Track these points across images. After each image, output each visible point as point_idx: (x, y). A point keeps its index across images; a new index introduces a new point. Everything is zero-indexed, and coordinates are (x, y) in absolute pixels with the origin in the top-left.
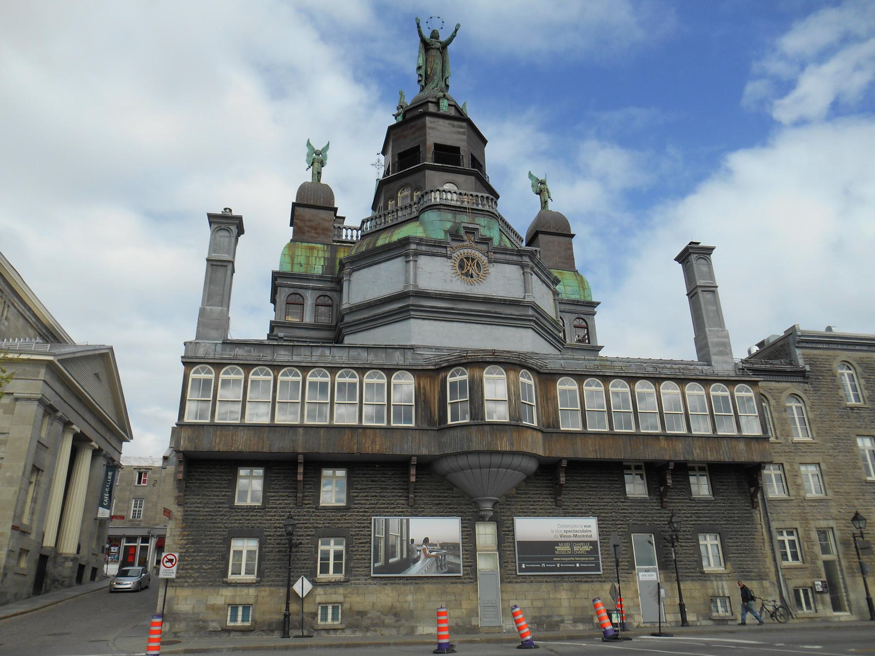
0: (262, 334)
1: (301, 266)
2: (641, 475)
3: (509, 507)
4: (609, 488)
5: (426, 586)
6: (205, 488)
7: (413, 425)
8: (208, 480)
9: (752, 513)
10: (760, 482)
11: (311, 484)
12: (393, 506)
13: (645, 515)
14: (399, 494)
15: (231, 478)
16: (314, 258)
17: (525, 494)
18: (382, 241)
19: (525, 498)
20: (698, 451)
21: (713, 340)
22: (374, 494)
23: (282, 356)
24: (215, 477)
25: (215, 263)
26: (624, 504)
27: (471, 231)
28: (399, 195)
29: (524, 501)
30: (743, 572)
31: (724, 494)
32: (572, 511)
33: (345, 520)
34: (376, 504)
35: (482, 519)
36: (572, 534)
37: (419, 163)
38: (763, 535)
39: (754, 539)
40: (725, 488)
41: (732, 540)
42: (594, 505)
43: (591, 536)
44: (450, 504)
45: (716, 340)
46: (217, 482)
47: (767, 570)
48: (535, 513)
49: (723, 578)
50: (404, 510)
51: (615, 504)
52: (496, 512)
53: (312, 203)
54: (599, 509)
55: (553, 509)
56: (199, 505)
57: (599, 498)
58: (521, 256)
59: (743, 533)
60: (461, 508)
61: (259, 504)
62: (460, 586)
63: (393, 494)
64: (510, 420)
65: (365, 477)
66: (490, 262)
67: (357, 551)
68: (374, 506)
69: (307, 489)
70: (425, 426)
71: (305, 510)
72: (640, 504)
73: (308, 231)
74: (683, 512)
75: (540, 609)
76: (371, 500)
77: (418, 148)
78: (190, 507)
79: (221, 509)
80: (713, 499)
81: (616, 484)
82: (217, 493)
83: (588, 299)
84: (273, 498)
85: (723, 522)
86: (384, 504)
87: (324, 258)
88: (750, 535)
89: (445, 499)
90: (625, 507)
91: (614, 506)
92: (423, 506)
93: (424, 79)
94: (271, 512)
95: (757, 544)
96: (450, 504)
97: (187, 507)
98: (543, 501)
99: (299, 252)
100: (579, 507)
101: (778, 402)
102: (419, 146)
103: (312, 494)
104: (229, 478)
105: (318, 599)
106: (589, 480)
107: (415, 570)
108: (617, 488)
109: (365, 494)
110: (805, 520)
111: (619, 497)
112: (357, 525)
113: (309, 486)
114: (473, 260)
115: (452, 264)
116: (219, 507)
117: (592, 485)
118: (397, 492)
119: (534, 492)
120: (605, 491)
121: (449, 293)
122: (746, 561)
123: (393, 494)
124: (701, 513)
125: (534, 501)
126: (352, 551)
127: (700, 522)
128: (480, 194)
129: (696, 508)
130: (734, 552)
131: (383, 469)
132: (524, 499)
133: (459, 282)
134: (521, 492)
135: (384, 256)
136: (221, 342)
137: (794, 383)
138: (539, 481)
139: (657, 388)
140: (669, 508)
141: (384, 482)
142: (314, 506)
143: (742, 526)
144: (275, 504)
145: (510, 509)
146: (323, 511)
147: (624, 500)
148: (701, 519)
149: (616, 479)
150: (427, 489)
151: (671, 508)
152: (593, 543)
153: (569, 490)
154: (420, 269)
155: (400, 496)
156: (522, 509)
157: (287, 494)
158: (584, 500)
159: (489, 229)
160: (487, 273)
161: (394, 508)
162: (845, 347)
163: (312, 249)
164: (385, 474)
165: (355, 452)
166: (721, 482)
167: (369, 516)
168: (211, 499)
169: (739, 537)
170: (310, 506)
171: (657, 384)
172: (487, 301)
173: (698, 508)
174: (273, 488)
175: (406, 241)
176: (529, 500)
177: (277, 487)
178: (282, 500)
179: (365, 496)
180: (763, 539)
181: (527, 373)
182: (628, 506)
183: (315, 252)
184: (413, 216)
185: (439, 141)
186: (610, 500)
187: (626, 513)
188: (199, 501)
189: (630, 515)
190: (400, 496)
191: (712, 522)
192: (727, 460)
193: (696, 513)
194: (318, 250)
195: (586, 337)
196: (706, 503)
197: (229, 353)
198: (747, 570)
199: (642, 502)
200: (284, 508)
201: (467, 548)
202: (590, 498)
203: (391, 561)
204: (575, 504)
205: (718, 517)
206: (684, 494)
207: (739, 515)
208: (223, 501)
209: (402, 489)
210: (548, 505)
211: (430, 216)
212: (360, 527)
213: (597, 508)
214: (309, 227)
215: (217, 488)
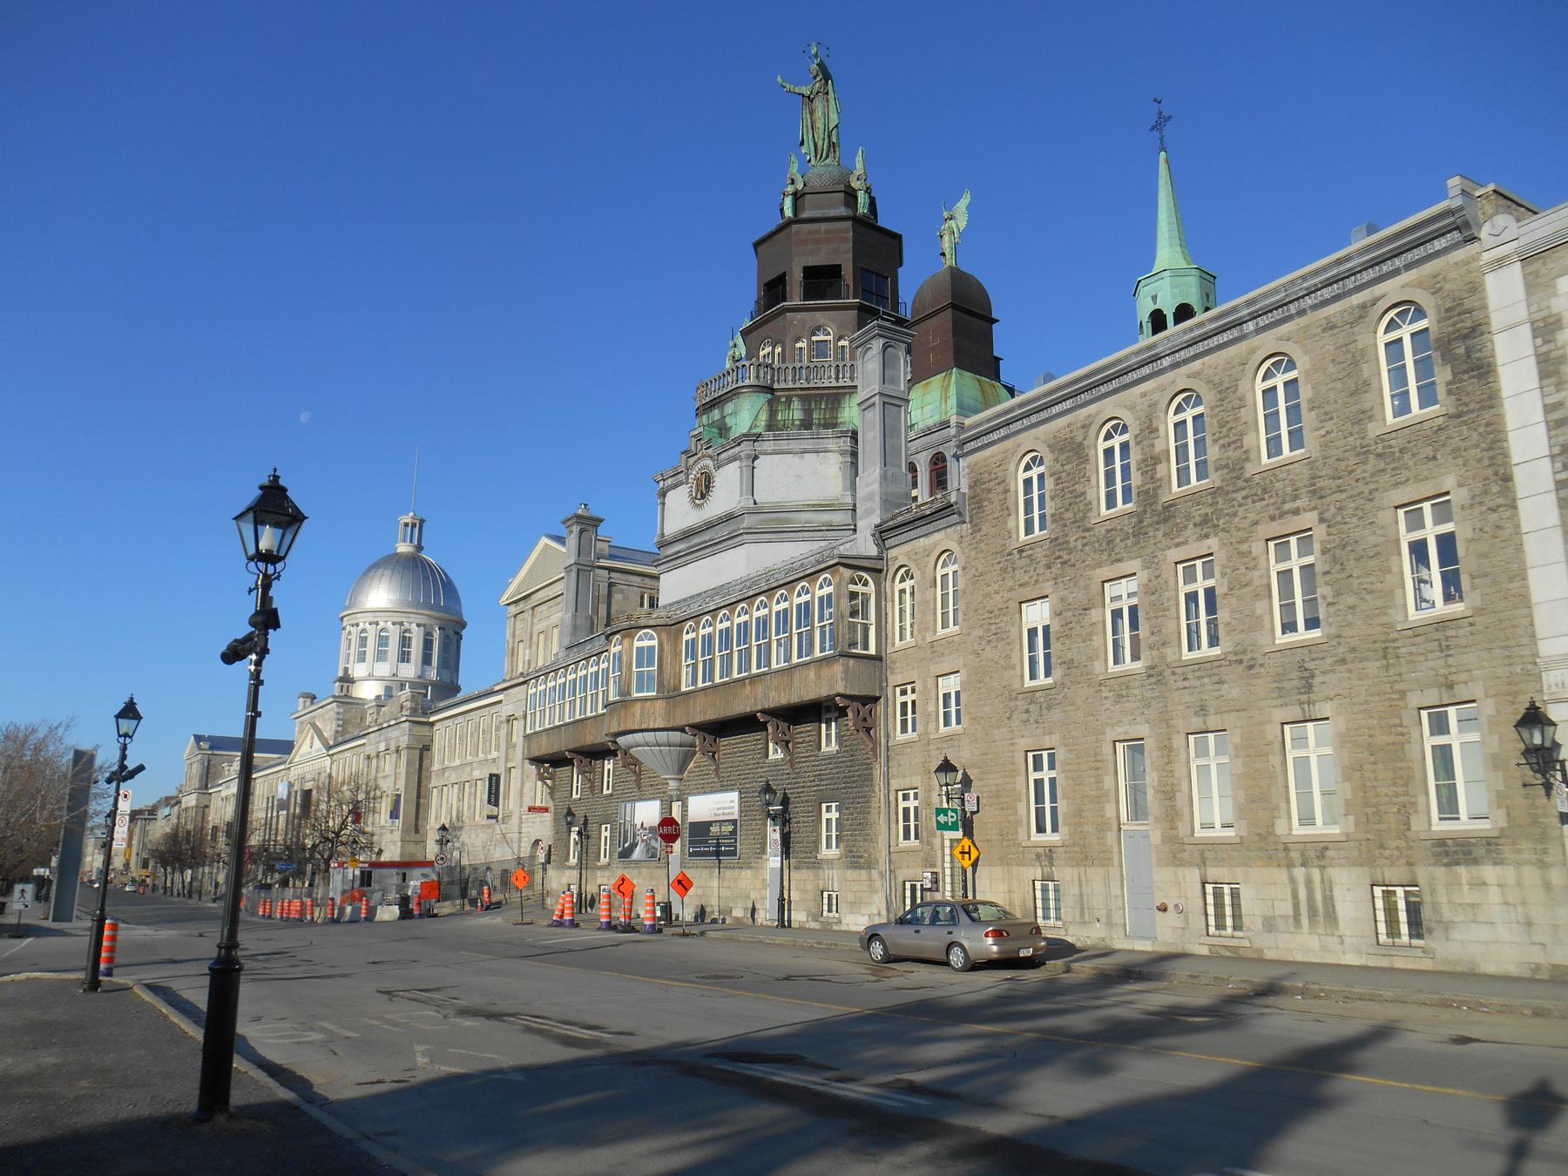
5: (643, 870)
9: (871, 769)
36: (721, 812)
43: (733, 814)
47: (878, 855)
51: (756, 771)
58: (739, 444)
62: (659, 870)
75: (700, 897)
105: (599, 881)
107: (637, 853)
130: (848, 827)
137: (949, 529)
152: (734, 822)
162: (1034, 419)
203: (626, 845)
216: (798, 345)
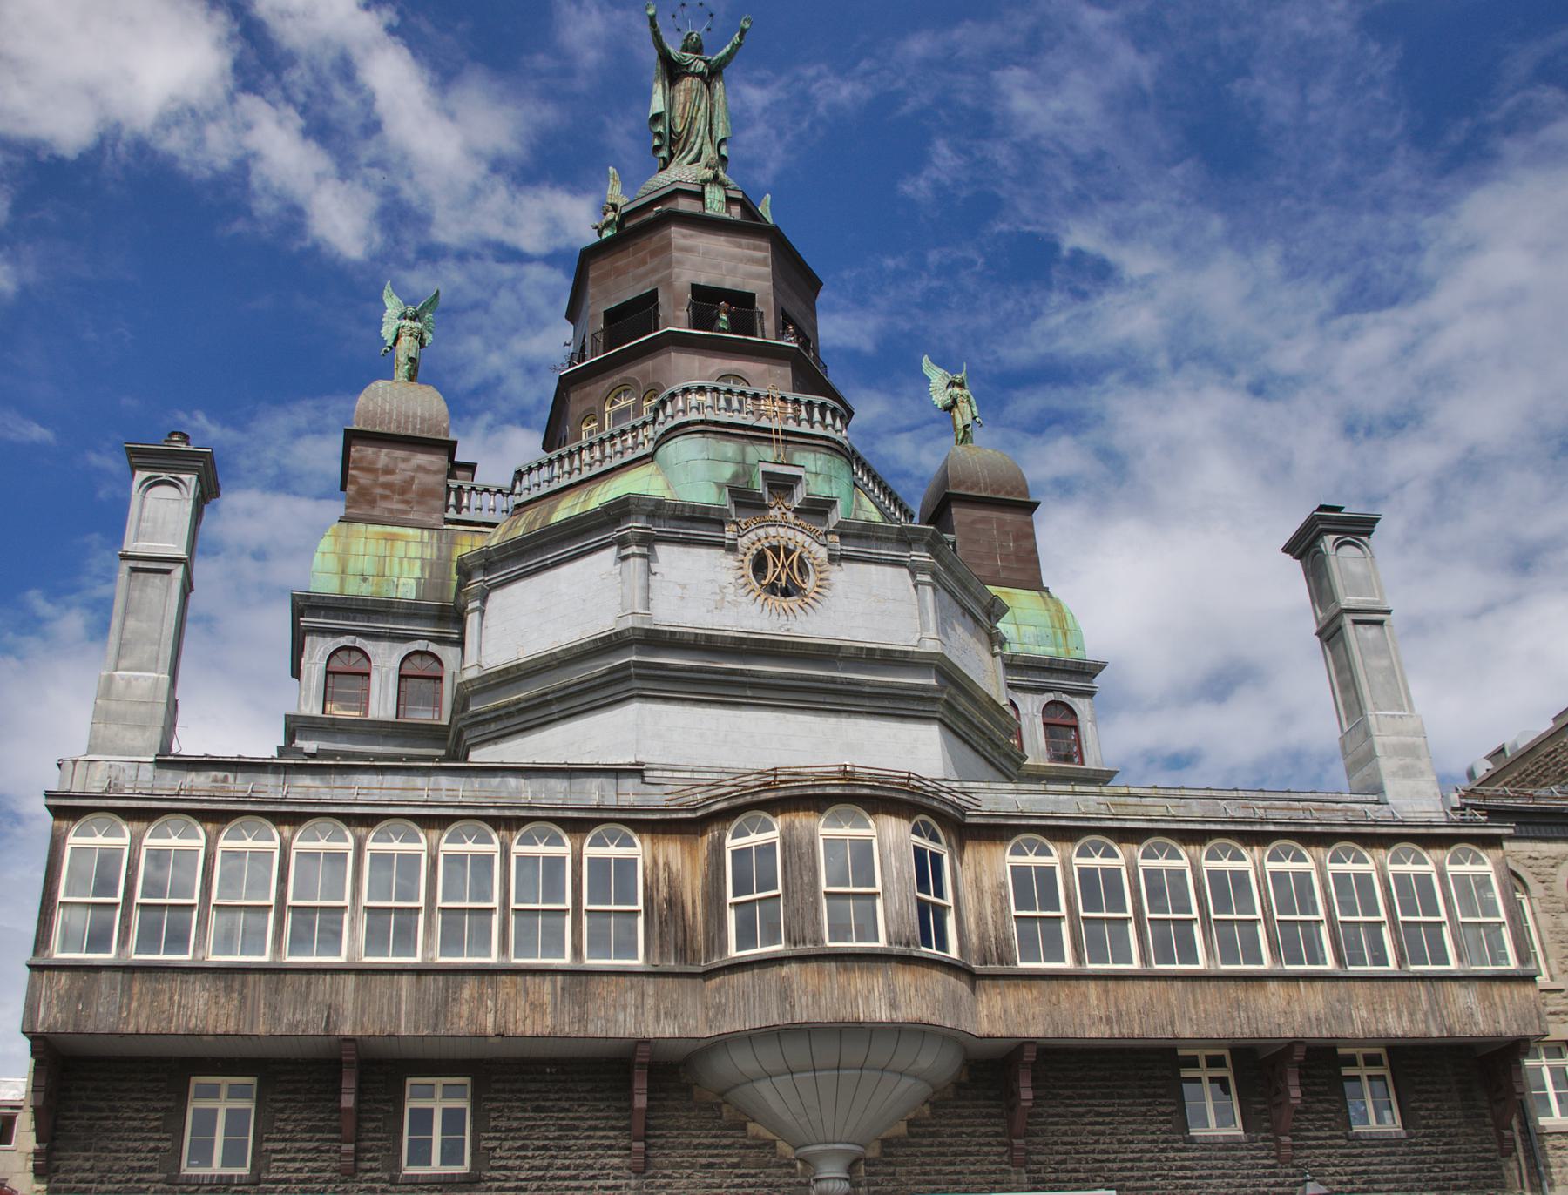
0: (265, 744)
1: (365, 580)
2: (1222, 1082)
3: (891, 1170)
4: (1145, 1114)
6: (106, 1130)
7: (638, 962)
8: (113, 1109)
9: (1500, 1168)
10: (1518, 1090)
11: (379, 1120)
12: (591, 1173)
13: (1237, 1181)
14: (607, 1142)
15: (171, 1104)
16: (396, 560)
17: (933, 1135)
18: (563, 511)
19: (932, 1145)
20: (1364, 1013)
21: (1385, 739)
22: (540, 1143)
23: (306, 788)
24: (131, 1103)
25: (141, 565)
26: (1183, 1155)
27: (782, 485)
28: (607, 409)
29: (929, 1154)
31: (1431, 1122)
32: (1053, 1176)
34: (547, 1168)
37: (656, 330)
40: (1432, 1105)
42: (1108, 1160)
45: (1394, 739)
46: (135, 1115)
48: (957, 1183)
50: (619, 1182)
51: (1162, 1156)
53: (393, 429)
54: (1120, 1170)
55: (1003, 1171)
56: (91, 1176)
57: (1120, 1142)
60: (768, 1176)
61: (245, 1171)
63: (590, 1142)
64: (889, 942)
65: (519, 1099)
66: (832, 559)
68: (541, 1173)
69: (368, 1131)
70: (672, 964)
71: (363, 1186)
72: (1223, 1154)
73: (384, 497)
74: (1332, 1169)
76: (533, 1157)
77: (653, 295)
78: (65, 1181)
79: (144, 1186)
80: (1403, 1134)
81: (1164, 1104)
82: (135, 1145)
83: (1076, 655)
84: (280, 1156)
86: (568, 1168)
87: (422, 559)
89: (726, 1152)
90: (1187, 1163)
91: (1159, 1160)
92: (669, 1172)
93: (667, 143)
97: (58, 1181)
98: (978, 1153)
99: (358, 546)
100: (1070, 1166)
102: (654, 293)
103: (380, 1143)
104: (165, 1104)
106: (1092, 1097)
108: (1163, 1114)
109: (520, 1143)
111: (1173, 1137)
113: (372, 1125)
114: (788, 553)
115: (737, 564)
116: (139, 1181)
117: (1102, 1110)
118: (602, 1138)
119: (955, 1130)
120: (1134, 1123)
121: (732, 634)
123: (590, 1142)
124: (1376, 1172)
125: (955, 1154)
128: (804, 398)
129: (1362, 1160)
131: (563, 1077)
132: (929, 1149)
134: (921, 1130)
135: (566, 550)
136: (152, 759)
138: (967, 1103)
140: (1295, 1162)
141: (568, 1110)
142: (386, 1176)
144: (286, 1170)
145: (893, 1174)
146: (408, 1188)
147: (1180, 1145)
148: (1376, 1187)
149: (1161, 1091)
150: (678, 1128)
151: (1301, 1162)
153: (1044, 1124)
154: (658, 577)
155: (610, 1147)
156: (925, 1174)
157: (316, 1144)
158: (1081, 1148)
159: (829, 478)
160: (823, 584)
161: (593, 1177)
163: (391, 538)
164: (571, 1091)
165: (490, 1031)
168: (119, 1158)
170: (375, 1175)
173: (1369, 1160)
174: (280, 1130)
175: (621, 509)
176: (942, 1149)
177: (289, 1128)
178: (303, 1160)
179: (519, 1149)
181: (930, 825)
182: (1193, 1159)
183: (400, 545)
184: (640, 452)
185: (702, 280)
186: (1147, 1146)
187: (1191, 1178)
188: (88, 1165)
189: (1199, 1182)
190: (610, 1147)
192: (1435, 1034)
193: (1365, 1172)
194: (407, 542)
195: (1075, 749)
196: (1385, 1145)
197: (172, 782)
199: (1228, 1150)
200: (309, 1180)
202: (1097, 1142)
204: (1058, 1157)
205: (1418, 1180)
206: (1333, 1124)
207: (1470, 1174)
208: (148, 1164)
209: (613, 1128)
210: (994, 1163)
211: (683, 450)
213: (1115, 1166)
214: (386, 486)
215: (135, 1130)
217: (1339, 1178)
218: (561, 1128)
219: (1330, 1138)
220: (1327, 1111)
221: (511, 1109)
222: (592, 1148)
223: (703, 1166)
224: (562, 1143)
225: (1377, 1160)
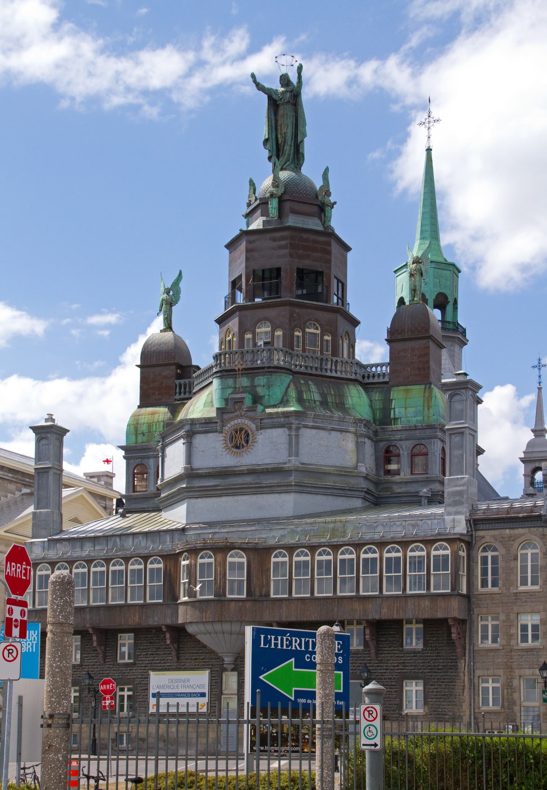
9: (457, 662)
12: (164, 662)
13: (357, 665)
30: (439, 714)
33: (132, 673)
34: (153, 660)
35: (225, 670)
38: (464, 682)
39: (454, 685)
40: (435, 639)
41: (433, 687)
44: (203, 659)
47: (462, 714)
49: (418, 720)
52: (237, 665)
58: (288, 417)
59: (444, 681)
67: (140, 695)
85: (427, 671)
88: (451, 682)
92: (185, 661)
94: (85, 668)
95: (457, 690)
96: (203, 659)
101: (509, 550)
109: (145, 653)
110: (509, 668)
112: (140, 677)
113: (108, 649)
122: (443, 705)
126: (137, 695)
127: (405, 671)
130: (433, 697)
133: (228, 456)
139: (358, 553)
142: (112, 663)
143: (444, 674)
166: (431, 634)
167: (148, 669)
169: (441, 684)
171: (358, 549)
172: (252, 472)
174: (87, 651)
179: (146, 655)
180: (464, 686)
191: (417, 671)
193: (403, 663)
198: (443, 713)
200: (94, 665)
201: (214, 693)
205: (423, 666)
206: (395, 645)
207: (444, 664)
212: (141, 678)
216: (297, 333)
217: (393, 664)
218: (157, 648)
219: (393, 650)
220: (394, 641)
221: (144, 643)
222: (165, 654)
223: (194, 659)
224: (157, 653)
225: (408, 658)
